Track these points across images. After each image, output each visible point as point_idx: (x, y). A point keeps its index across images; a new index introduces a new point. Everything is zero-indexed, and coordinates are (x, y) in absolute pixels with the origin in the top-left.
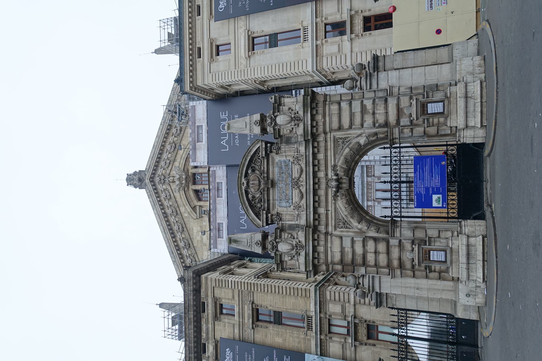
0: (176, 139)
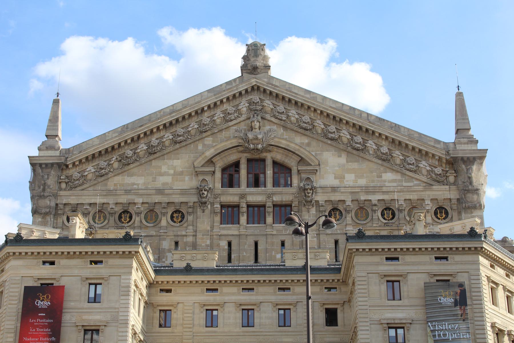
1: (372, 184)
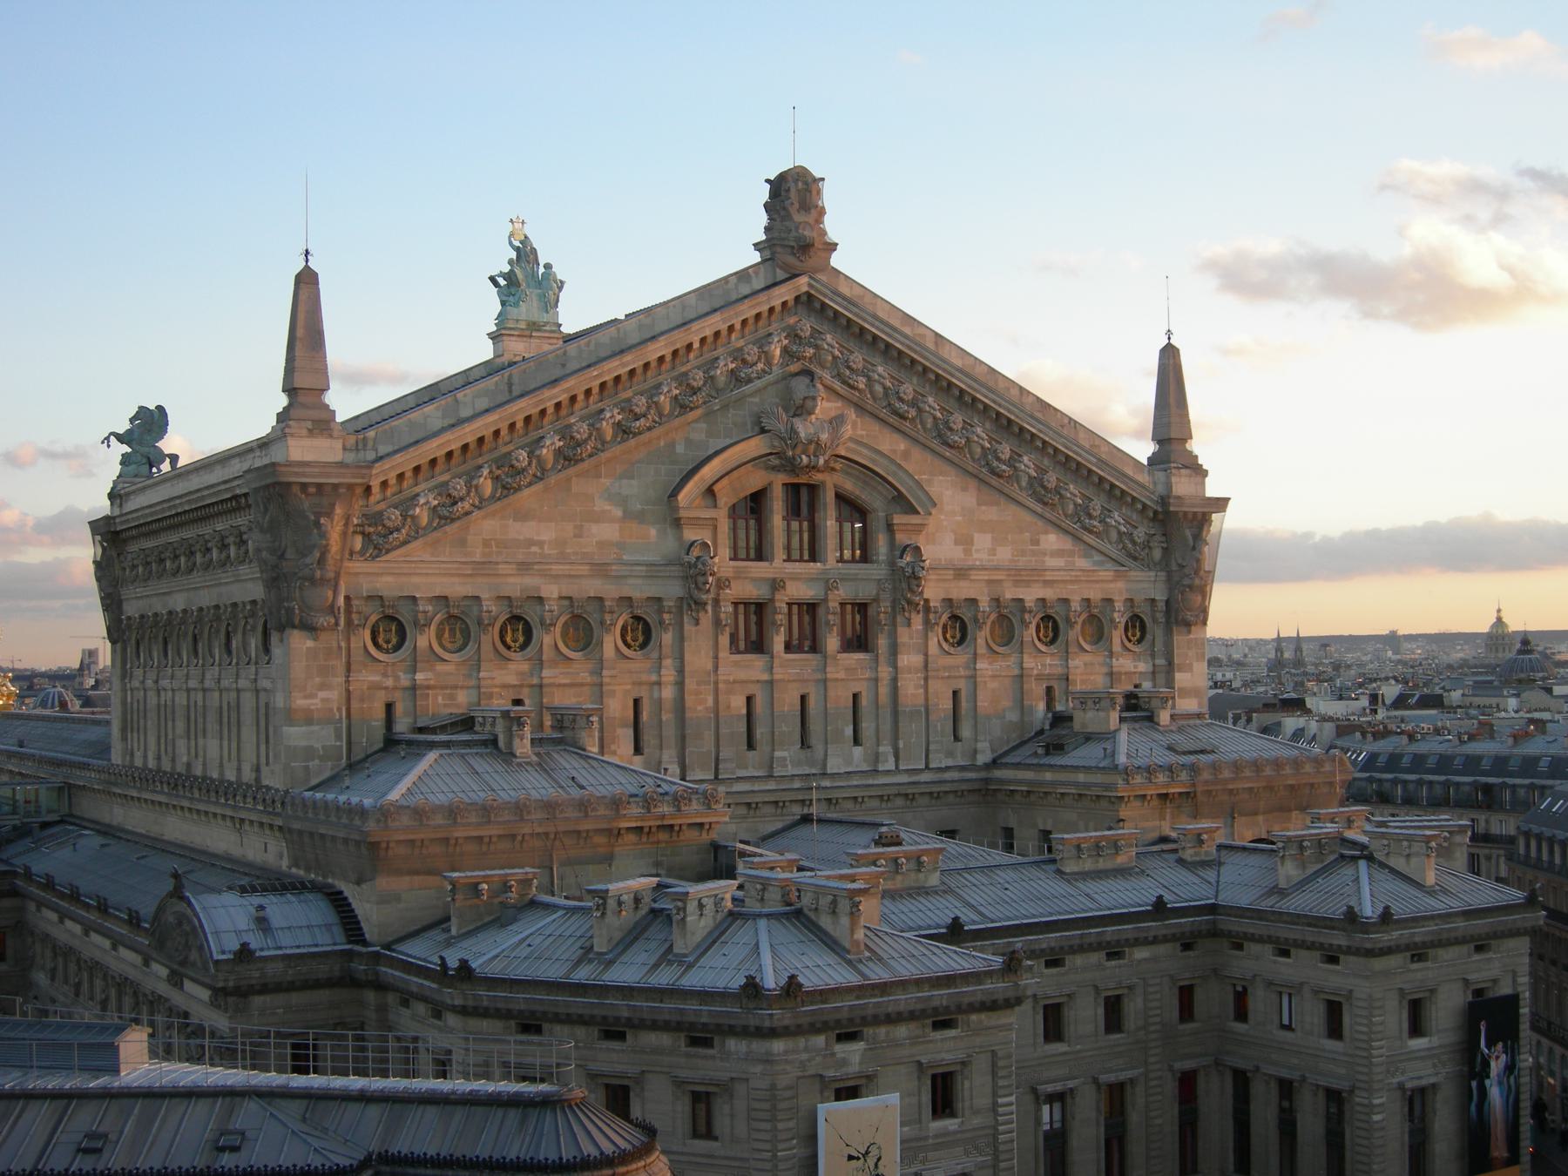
0: (929, 423)
1: (1022, 562)
